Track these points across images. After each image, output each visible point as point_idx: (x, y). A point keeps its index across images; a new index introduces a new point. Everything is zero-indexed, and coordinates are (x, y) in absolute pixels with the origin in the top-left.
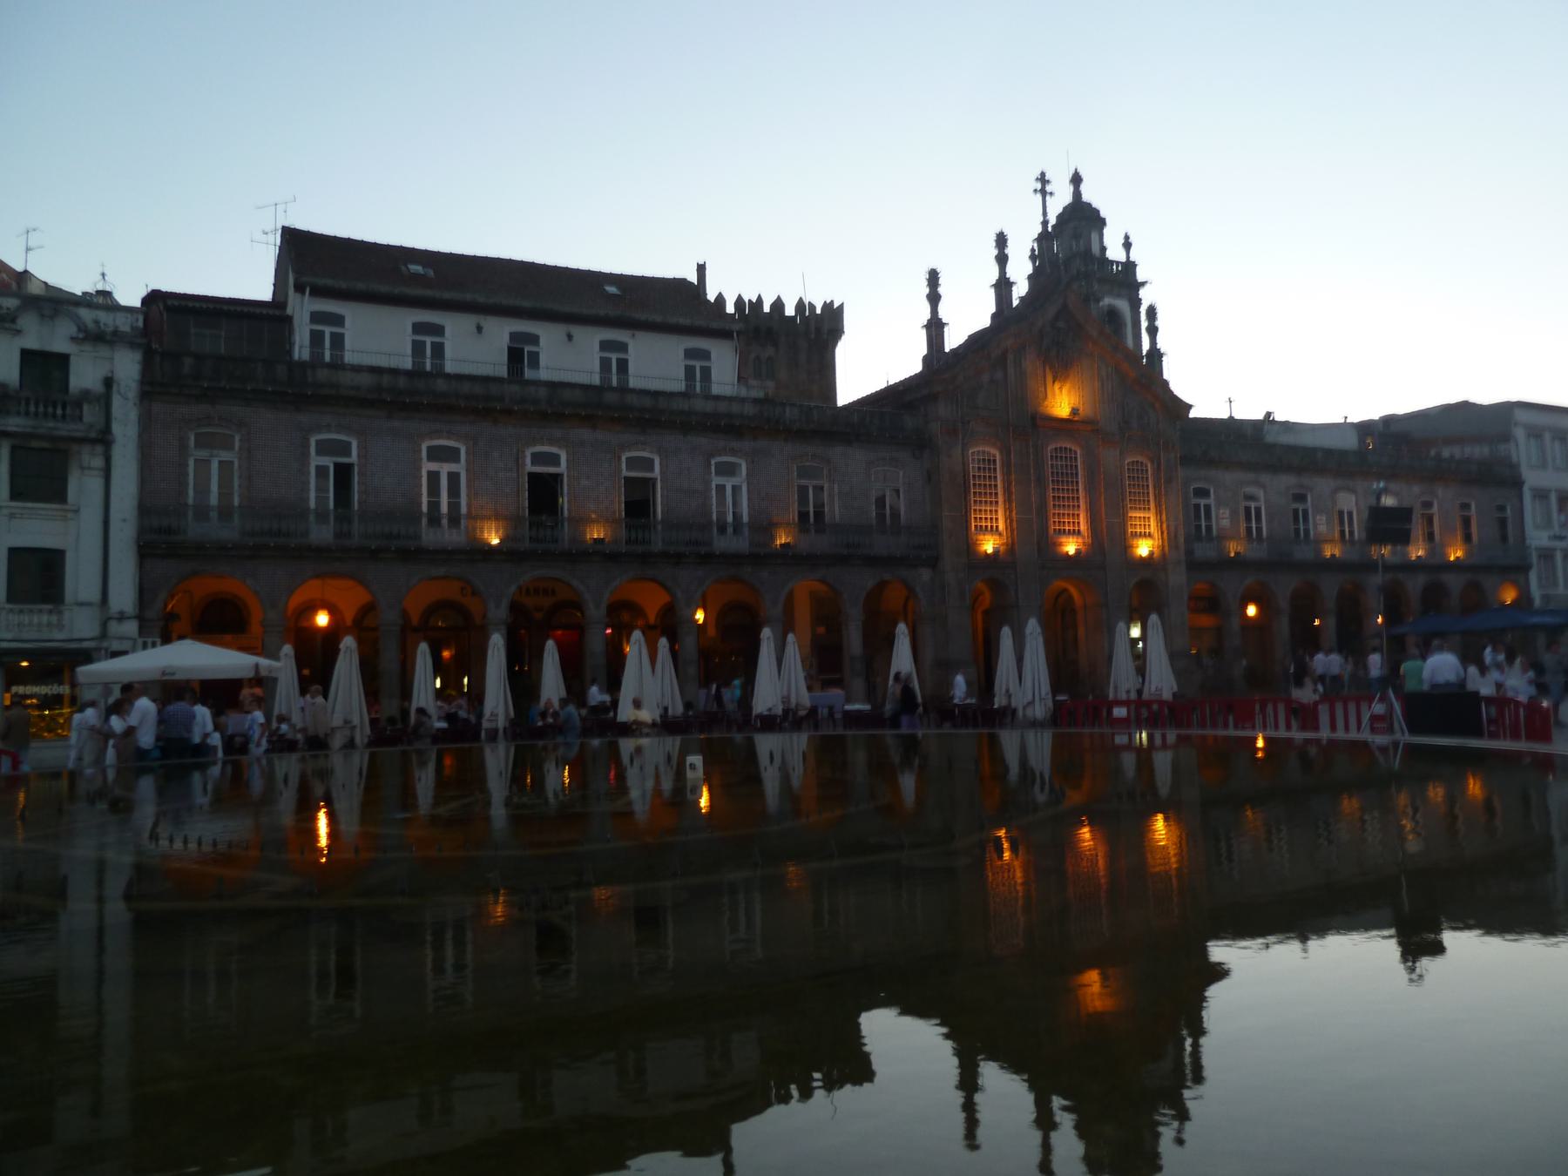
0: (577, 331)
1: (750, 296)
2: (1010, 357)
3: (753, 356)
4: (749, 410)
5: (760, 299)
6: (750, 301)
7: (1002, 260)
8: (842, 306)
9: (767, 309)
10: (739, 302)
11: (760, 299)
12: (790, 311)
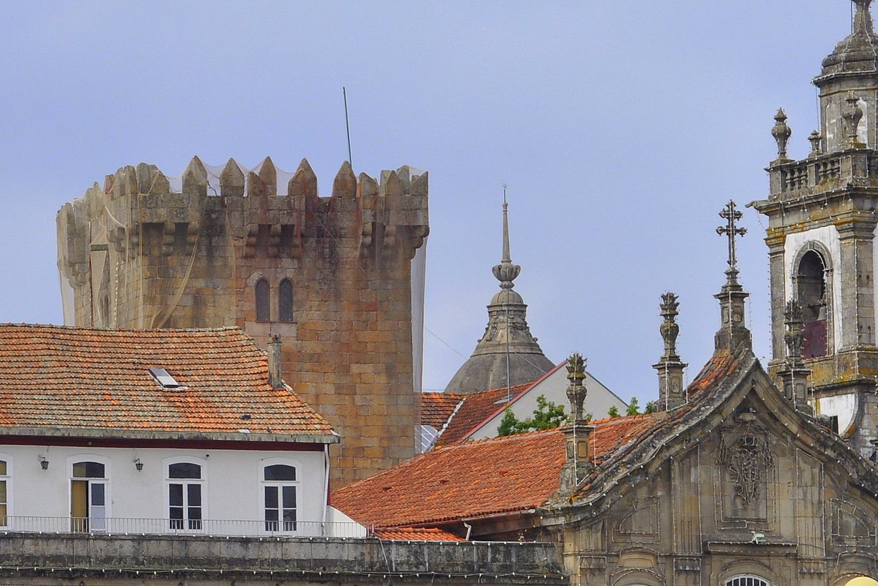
0: (146, 455)
1: (251, 164)
2: (676, 466)
3: (256, 276)
4: (349, 554)
5: (269, 168)
6: (252, 174)
7: (671, 334)
8: (425, 177)
9: (282, 189)
10: (230, 174)
11: (269, 168)
12: (325, 190)
